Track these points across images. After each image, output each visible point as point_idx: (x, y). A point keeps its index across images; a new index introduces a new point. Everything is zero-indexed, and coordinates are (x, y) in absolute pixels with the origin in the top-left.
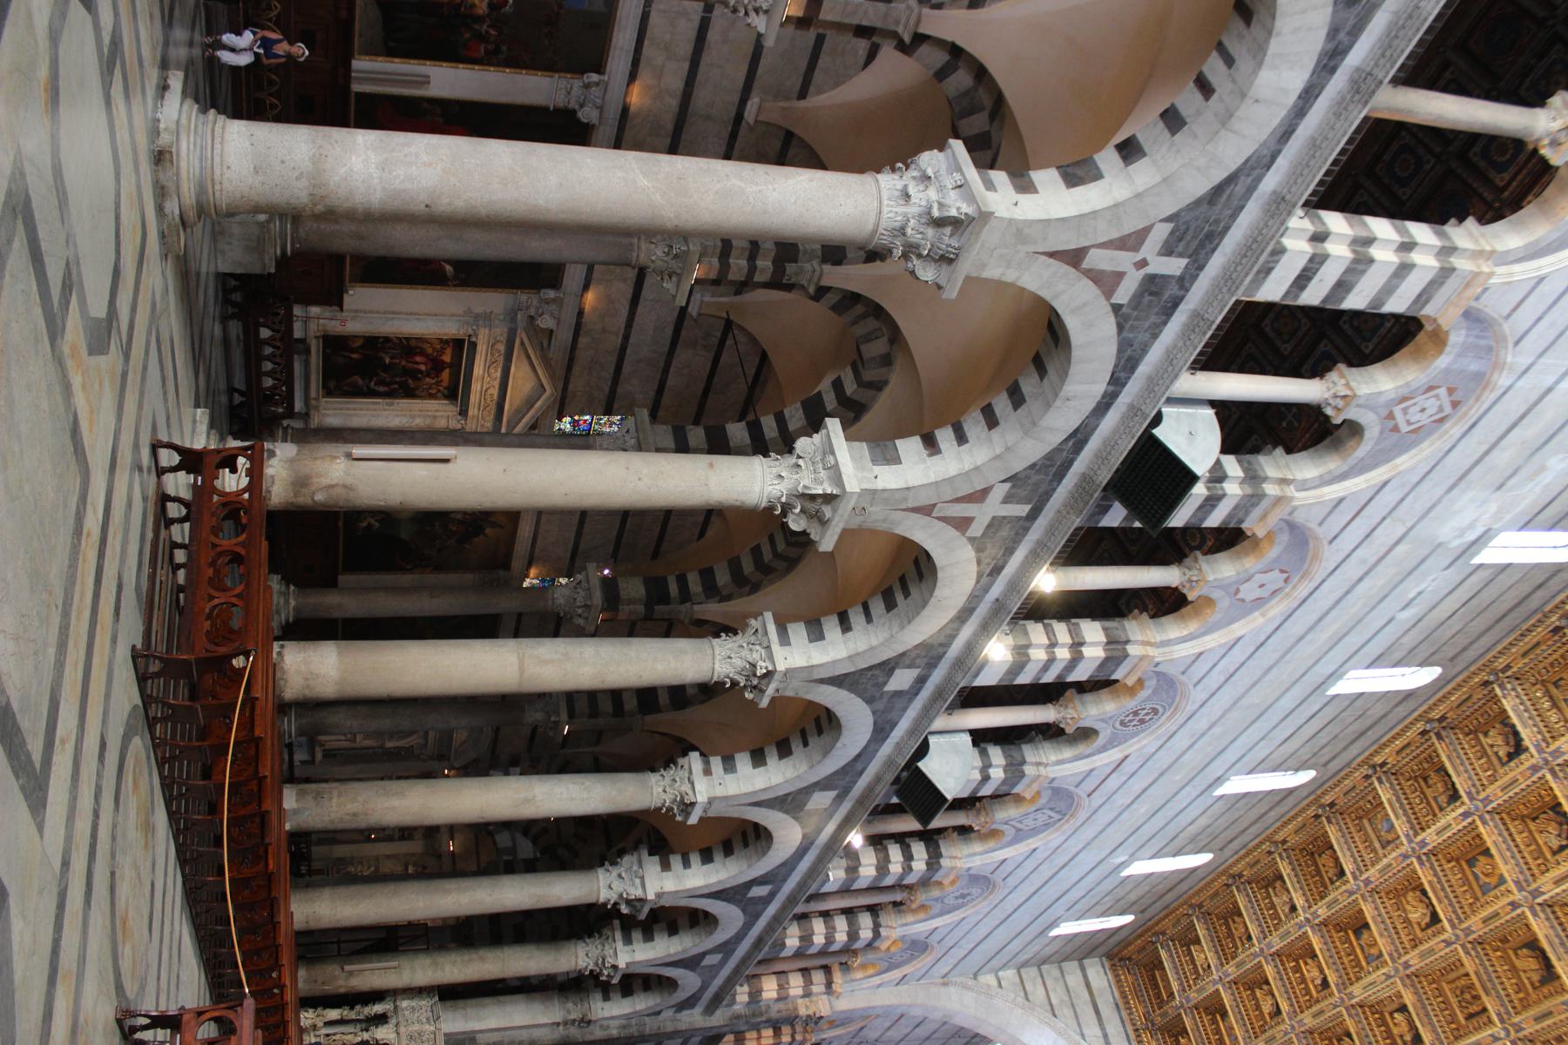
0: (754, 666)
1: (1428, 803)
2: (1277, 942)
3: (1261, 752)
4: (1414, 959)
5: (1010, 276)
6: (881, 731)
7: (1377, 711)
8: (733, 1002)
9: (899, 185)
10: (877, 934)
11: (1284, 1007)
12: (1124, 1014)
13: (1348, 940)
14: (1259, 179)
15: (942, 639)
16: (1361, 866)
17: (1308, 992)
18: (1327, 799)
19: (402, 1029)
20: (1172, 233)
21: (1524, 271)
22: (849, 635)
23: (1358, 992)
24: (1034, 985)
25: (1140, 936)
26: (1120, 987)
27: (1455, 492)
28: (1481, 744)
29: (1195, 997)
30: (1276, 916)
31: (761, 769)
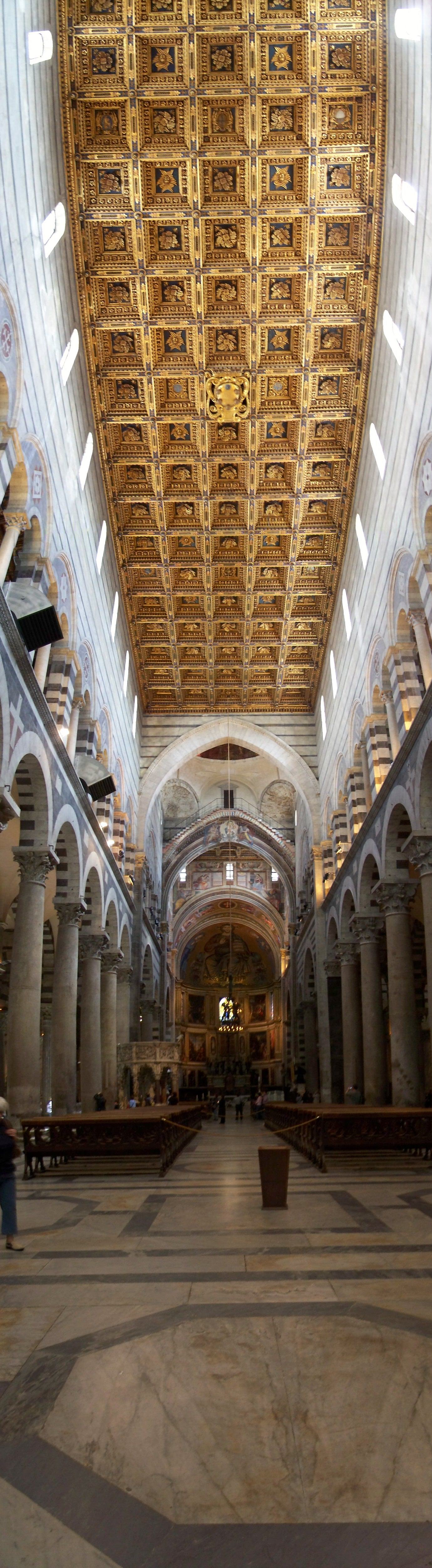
2: (173, 638)
4: (209, 586)
6: (72, 802)
10: (122, 822)
11: (200, 645)
12: (172, 714)
13: (185, 607)
16: (162, 590)
22: (36, 807)
23: (210, 613)
26: (159, 712)
29: (178, 681)
30: (161, 633)
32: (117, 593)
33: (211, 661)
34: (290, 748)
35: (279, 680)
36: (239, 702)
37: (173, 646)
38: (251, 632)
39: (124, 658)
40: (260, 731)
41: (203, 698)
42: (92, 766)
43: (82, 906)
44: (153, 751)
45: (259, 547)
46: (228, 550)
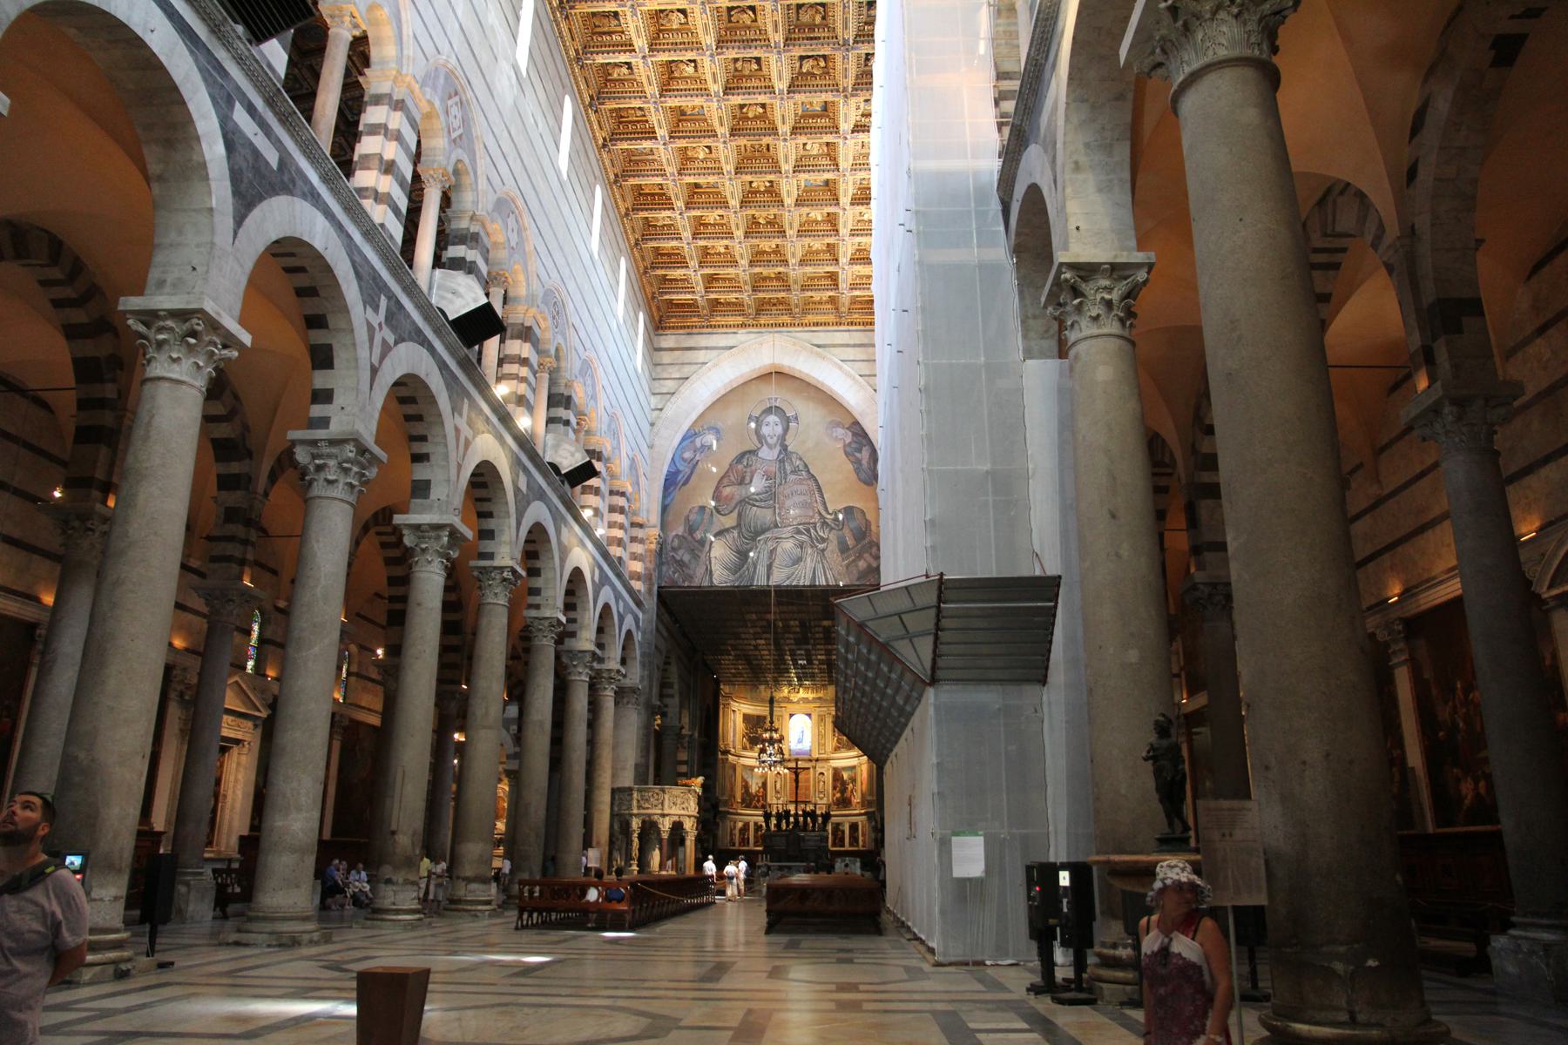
0: (505, 580)
1: (638, 122)
2: (687, 235)
5: (377, 415)
6: (542, 496)
7: (578, 141)
8: (639, 591)
9: (321, 482)
10: (623, 494)
12: (695, 331)
14: (356, 245)
15: (510, 456)
17: (722, 225)
18: (612, 177)
19: (635, 811)
20: (371, 306)
21: (410, 49)
22: (495, 514)
23: (734, 203)
24: (664, 386)
25: (650, 308)
26: (677, 327)
27: (495, 94)
28: (617, 80)
29: (700, 288)
30: (669, 226)
31: (542, 571)
33: (743, 262)
34: (860, 378)
35: (842, 285)
36: (789, 312)
37: (686, 244)
38: (796, 226)
39: (616, 271)
40: (818, 355)
41: (737, 307)
42: (567, 446)
43: (558, 620)
44: (669, 385)
45: (796, 115)
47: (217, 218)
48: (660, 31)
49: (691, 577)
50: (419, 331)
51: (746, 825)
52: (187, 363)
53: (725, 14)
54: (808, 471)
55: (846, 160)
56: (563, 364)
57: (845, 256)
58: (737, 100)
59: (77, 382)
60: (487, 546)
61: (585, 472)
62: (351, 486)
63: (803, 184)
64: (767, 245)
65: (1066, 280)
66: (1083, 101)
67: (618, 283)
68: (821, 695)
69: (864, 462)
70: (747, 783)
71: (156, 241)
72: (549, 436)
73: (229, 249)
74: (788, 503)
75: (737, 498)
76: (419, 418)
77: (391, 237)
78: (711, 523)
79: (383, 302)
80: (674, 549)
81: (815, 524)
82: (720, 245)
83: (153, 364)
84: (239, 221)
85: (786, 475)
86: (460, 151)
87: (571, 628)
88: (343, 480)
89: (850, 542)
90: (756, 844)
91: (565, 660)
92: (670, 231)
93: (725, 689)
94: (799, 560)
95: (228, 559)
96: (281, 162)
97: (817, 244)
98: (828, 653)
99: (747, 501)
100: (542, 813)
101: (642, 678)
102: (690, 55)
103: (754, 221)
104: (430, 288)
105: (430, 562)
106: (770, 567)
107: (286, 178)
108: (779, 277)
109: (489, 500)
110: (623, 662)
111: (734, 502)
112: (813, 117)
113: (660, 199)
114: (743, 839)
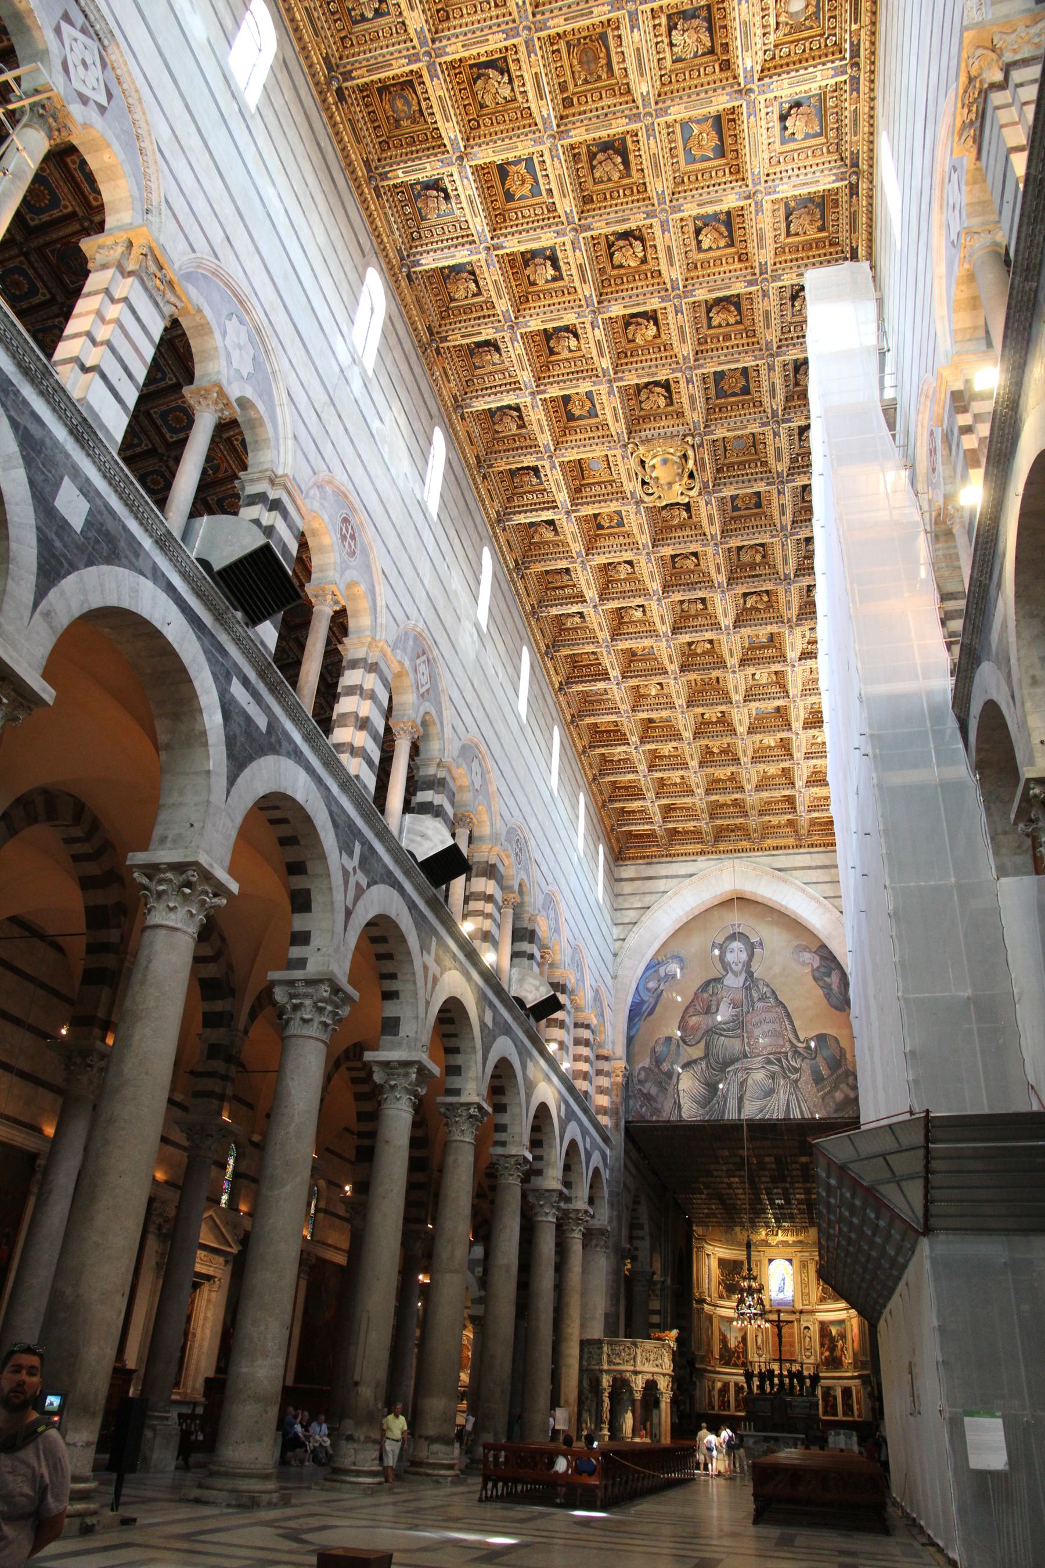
0: (471, 1116)
2: (643, 768)
3: (542, 766)
5: (350, 956)
6: (507, 1031)
7: (536, 687)
9: (298, 1021)
10: (587, 1026)
12: (654, 860)
17: (677, 756)
18: (569, 718)
19: (605, 1367)
21: (383, 618)
23: (687, 734)
29: (658, 818)
30: (625, 760)
32: (556, 728)
35: (800, 809)
36: (748, 837)
37: (643, 777)
38: (750, 753)
39: (575, 806)
40: (780, 878)
42: (531, 980)
43: (525, 1158)
44: (631, 915)
45: (743, 648)
46: (700, 655)
47: (213, 779)
48: (610, 581)
49: (658, 1111)
50: (390, 874)
51: (726, 1385)
52: (182, 912)
53: (669, 561)
54: (776, 998)
55: (796, 687)
56: (526, 899)
57: (801, 779)
58: (685, 638)
59: (89, 927)
60: (455, 1082)
61: (549, 1007)
62: (325, 1025)
63: (754, 713)
64: (722, 773)
65: (1036, 796)
66: (1032, 616)
67: (577, 817)
68: (801, 1238)
69: (835, 987)
70: (725, 1337)
71: (161, 802)
72: (514, 970)
73: (223, 806)
74: (757, 1031)
75: (704, 1028)
76: (389, 956)
77: (365, 787)
78: (678, 1054)
79: (357, 848)
80: (640, 1081)
81: (786, 1053)
82: (675, 776)
83: (153, 913)
84: (232, 780)
85: (753, 1002)
86: (427, 704)
87: (538, 1165)
88: (318, 1019)
89: (825, 1072)
90: (738, 1408)
91: (531, 1199)
92: (627, 765)
93: (698, 1230)
94: (770, 1092)
95: (209, 1094)
96: (270, 726)
97: (772, 769)
98: (808, 1191)
99: (714, 1031)
100: (508, 1366)
101: (610, 1217)
102: (638, 601)
103: (708, 751)
104: (401, 832)
105: (398, 1099)
106: (741, 1100)
107: (273, 739)
108: (736, 803)
109: (455, 1036)
110: (591, 1201)
111: (699, 1034)
112: (760, 648)
113: (616, 735)
114: (723, 1402)
